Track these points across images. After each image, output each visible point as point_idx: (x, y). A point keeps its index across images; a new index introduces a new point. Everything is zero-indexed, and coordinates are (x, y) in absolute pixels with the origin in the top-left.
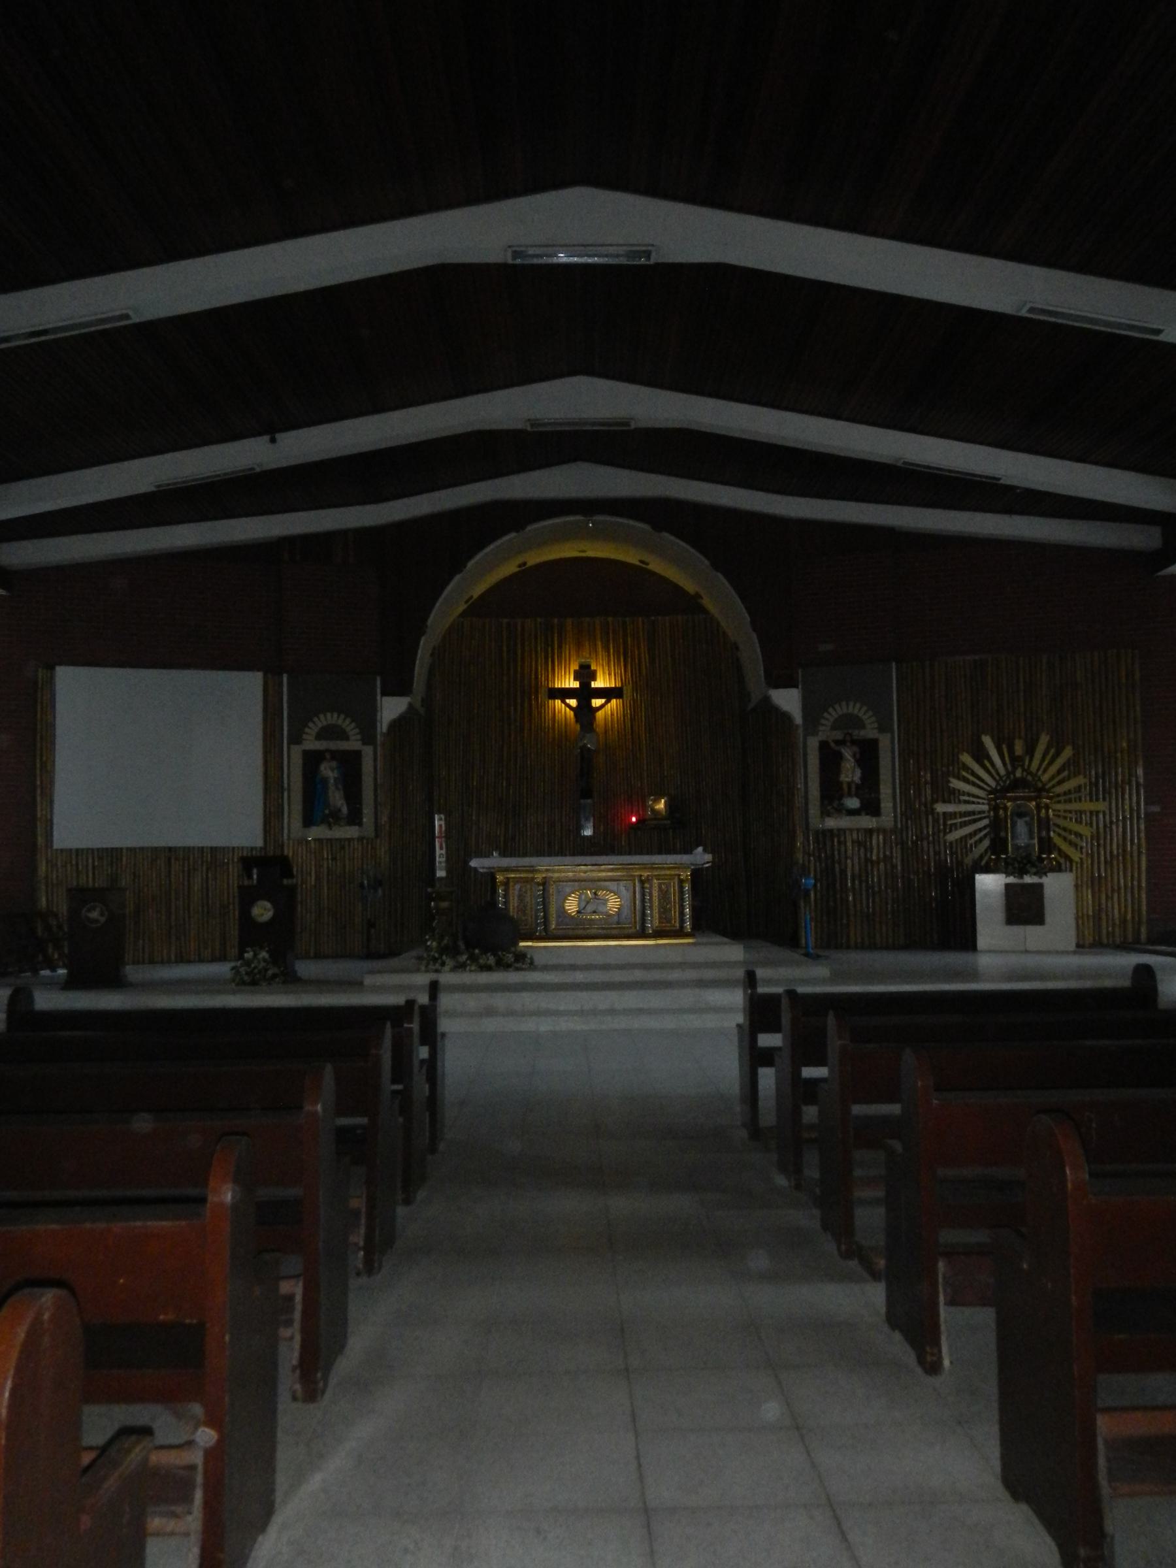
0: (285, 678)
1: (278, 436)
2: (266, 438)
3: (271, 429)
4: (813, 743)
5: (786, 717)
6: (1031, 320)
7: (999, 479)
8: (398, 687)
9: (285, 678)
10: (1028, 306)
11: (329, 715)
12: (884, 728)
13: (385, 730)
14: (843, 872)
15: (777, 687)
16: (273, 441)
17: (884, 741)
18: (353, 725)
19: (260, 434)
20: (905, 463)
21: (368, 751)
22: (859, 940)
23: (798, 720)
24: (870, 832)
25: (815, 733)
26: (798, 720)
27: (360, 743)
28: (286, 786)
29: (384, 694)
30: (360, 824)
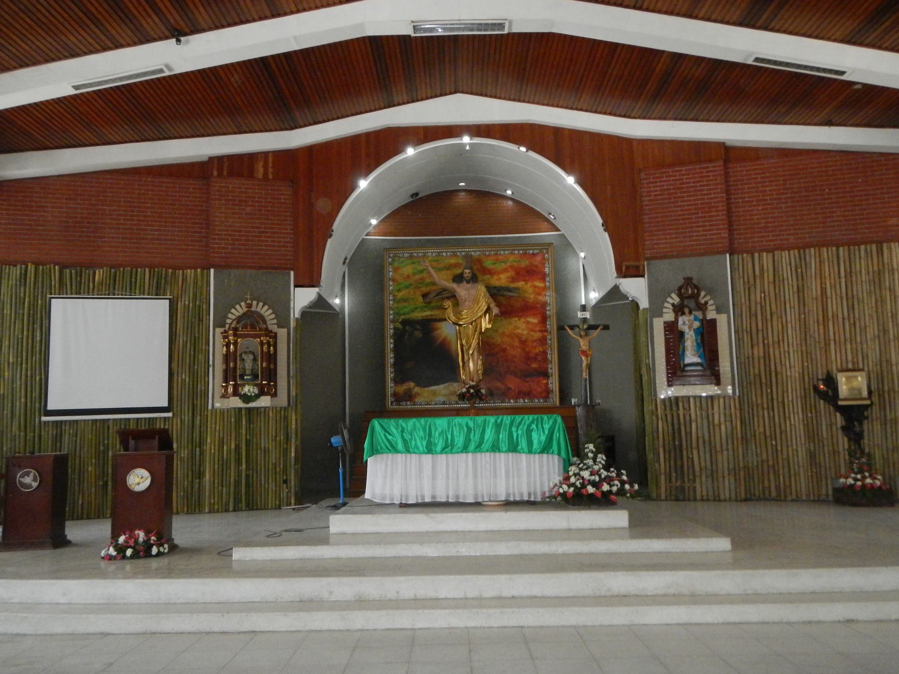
0: (212, 270)
1: (182, 39)
2: (174, 40)
3: (178, 34)
4: (658, 325)
5: (635, 304)
6: (756, 66)
7: (842, 73)
8: (310, 279)
9: (212, 270)
10: (753, 58)
11: (273, 316)
12: (719, 311)
13: (297, 315)
14: (689, 434)
15: (624, 277)
16: (178, 41)
17: (722, 321)
18: (270, 311)
19: (167, 38)
20: (757, 60)
21: (282, 333)
22: (704, 493)
23: (644, 303)
24: (711, 398)
25: (660, 315)
26: (644, 303)
27: (276, 326)
28: (211, 363)
29: (296, 286)
30: (275, 395)
